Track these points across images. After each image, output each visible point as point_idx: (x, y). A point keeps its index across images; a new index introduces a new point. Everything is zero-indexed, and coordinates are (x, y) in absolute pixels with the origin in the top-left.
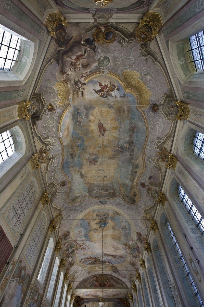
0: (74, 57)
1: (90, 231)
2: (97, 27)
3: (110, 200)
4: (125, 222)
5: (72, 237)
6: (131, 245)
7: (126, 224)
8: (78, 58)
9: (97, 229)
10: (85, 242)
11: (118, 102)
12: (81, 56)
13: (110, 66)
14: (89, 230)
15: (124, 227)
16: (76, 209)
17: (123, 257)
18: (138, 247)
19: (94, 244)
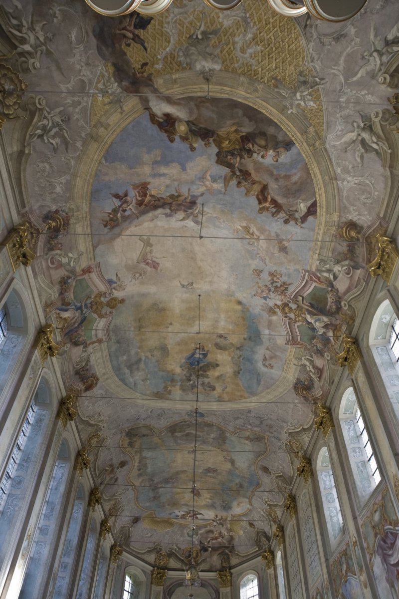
0: (219, 540)
1: (238, 348)
2: (197, 565)
3: (182, 418)
4: (135, 384)
5: (296, 362)
6: (98, 319)
7: (131, 380)
8: (216, 538)
9: (215, 349)
10: (265, 315)
11: (177, 509)
12: (213, 539)
13: (187, 530)
14: (241, 353)
15: (135, 367)
16: (258, 422)
17: (105, 226)
18: (76, 344)
19: (234, 292)
